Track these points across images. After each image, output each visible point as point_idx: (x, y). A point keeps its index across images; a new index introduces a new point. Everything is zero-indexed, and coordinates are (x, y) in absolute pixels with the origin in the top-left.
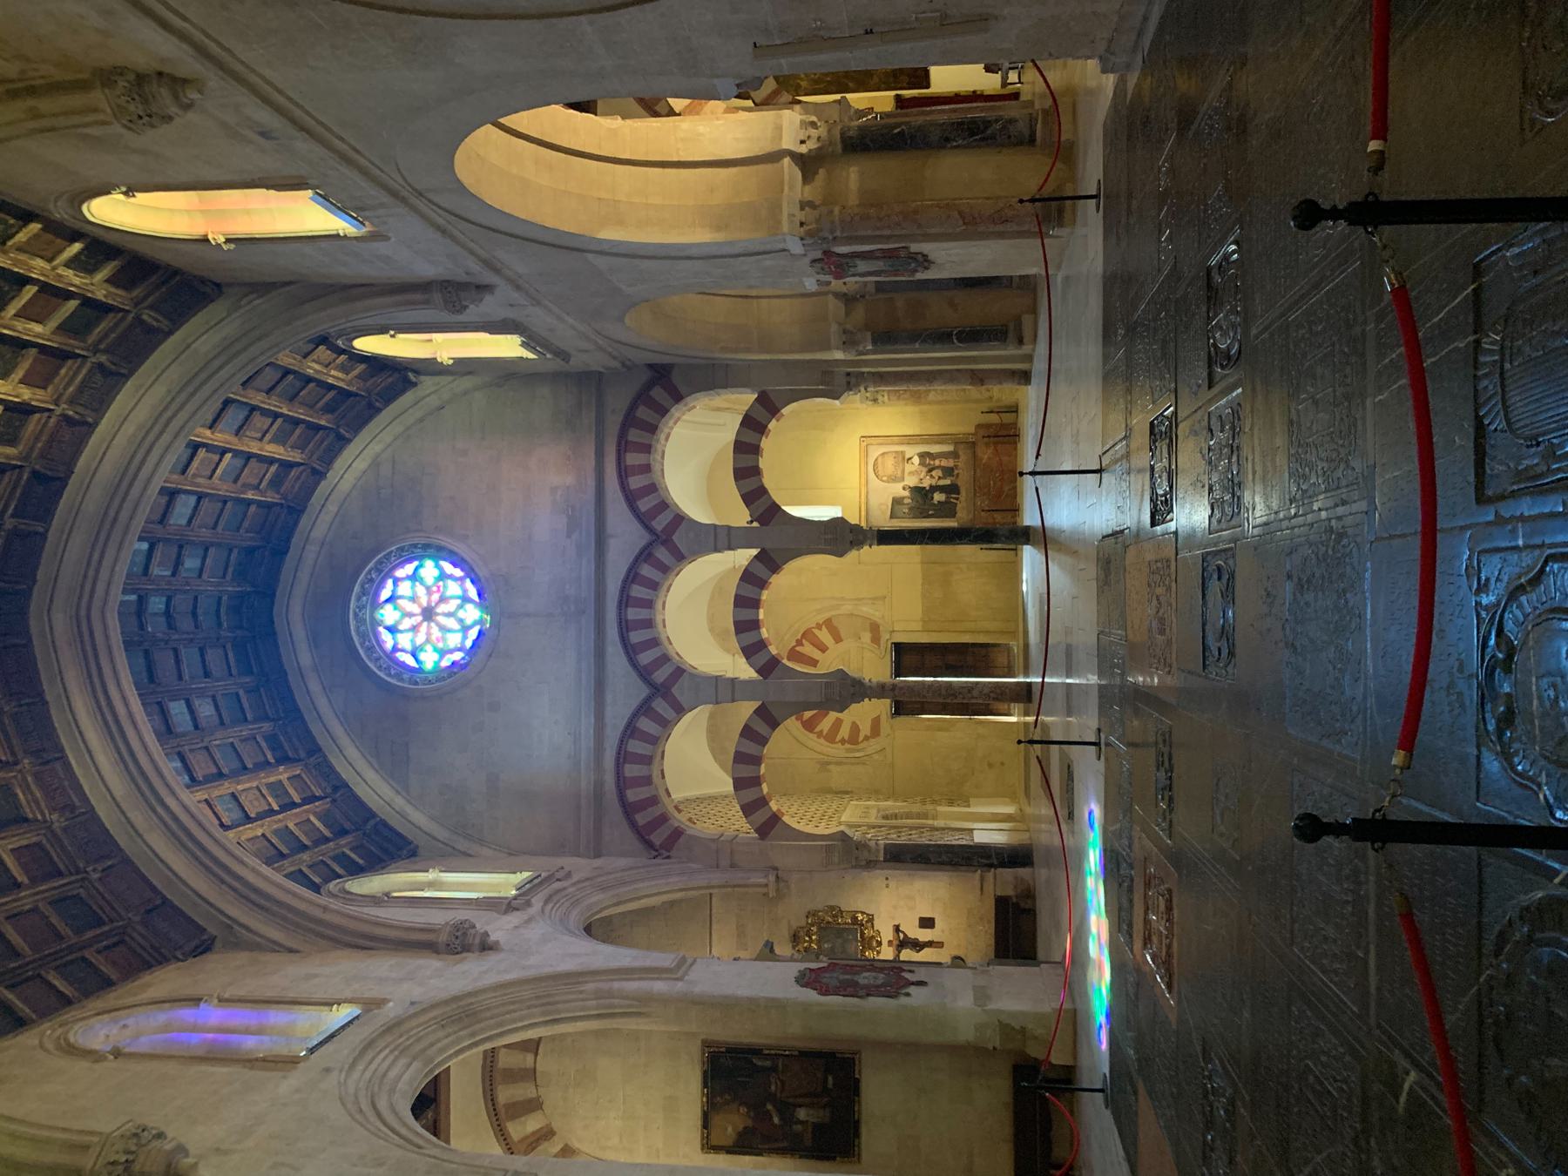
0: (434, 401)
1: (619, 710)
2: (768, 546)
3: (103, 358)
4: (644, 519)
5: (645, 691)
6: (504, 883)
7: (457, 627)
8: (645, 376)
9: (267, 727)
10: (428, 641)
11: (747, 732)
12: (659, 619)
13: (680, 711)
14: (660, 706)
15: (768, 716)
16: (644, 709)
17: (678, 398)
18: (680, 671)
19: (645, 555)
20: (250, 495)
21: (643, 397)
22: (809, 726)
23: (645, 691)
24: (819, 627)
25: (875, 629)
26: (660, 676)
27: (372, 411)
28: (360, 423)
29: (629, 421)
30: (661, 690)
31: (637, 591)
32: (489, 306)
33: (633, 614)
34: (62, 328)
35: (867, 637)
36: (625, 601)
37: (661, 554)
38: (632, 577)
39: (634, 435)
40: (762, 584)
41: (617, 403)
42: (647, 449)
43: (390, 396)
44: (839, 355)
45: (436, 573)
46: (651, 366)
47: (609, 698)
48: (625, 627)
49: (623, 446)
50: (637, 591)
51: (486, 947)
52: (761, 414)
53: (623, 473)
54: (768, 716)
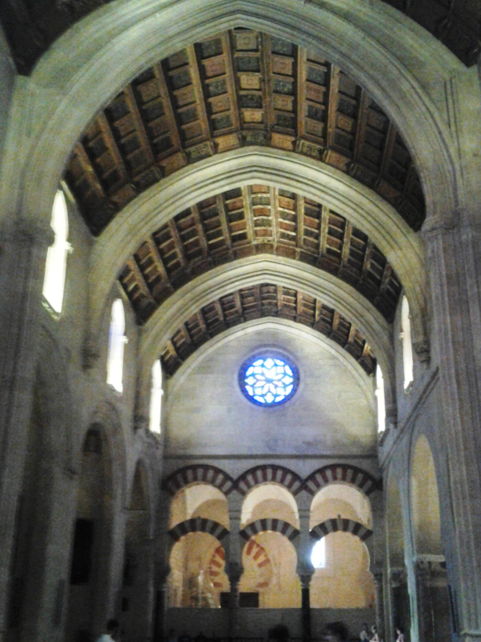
0: (362, 383)
1: (226, 466)
2: (302, 536)
3: (361, 282)
4: (312, 477)
5: (235, 477)
6: (155, 426)
7: (264, 393)
8: (376, 476)
9: (222, 319)
10: (258, 380)
11: (216, 525)
12: (268, 483)
13: (226, 493)
14: (229, 484)
15: (223, 535)
16: (227, 477)
17: (367, 493)
18: (244, 494)
19: (296, 477)
20: (317, 312)
21: (367, 476)
22: (218, 551)
23: (235, 477)
24: (266, 556)
25: (264, 584)
26: (242, 485)
27: (357, 357)
28: (350, 351)
29: (357, 470)
30: (235, 485)
31: (279, 473)
32: (391, 426)
33: (269, 472)
34: (369, 274)
35: (261, 580)
36: (275, 468)
37: (297, 484)
38: (286, 471)
39: (350, 473)
40: (283, 532)
41: (365, 465)
42: (344, 479)
43: (363, 365)
44: (389, 571)
45: (287, 383)
46: (381, 480)
47: (232, 461)
48: (263, 468)
49: (345, 467)
50: (279, 473)
51: (135, 428)
52: (362, 532)
53: (333, 467)
54: (223, 535)
